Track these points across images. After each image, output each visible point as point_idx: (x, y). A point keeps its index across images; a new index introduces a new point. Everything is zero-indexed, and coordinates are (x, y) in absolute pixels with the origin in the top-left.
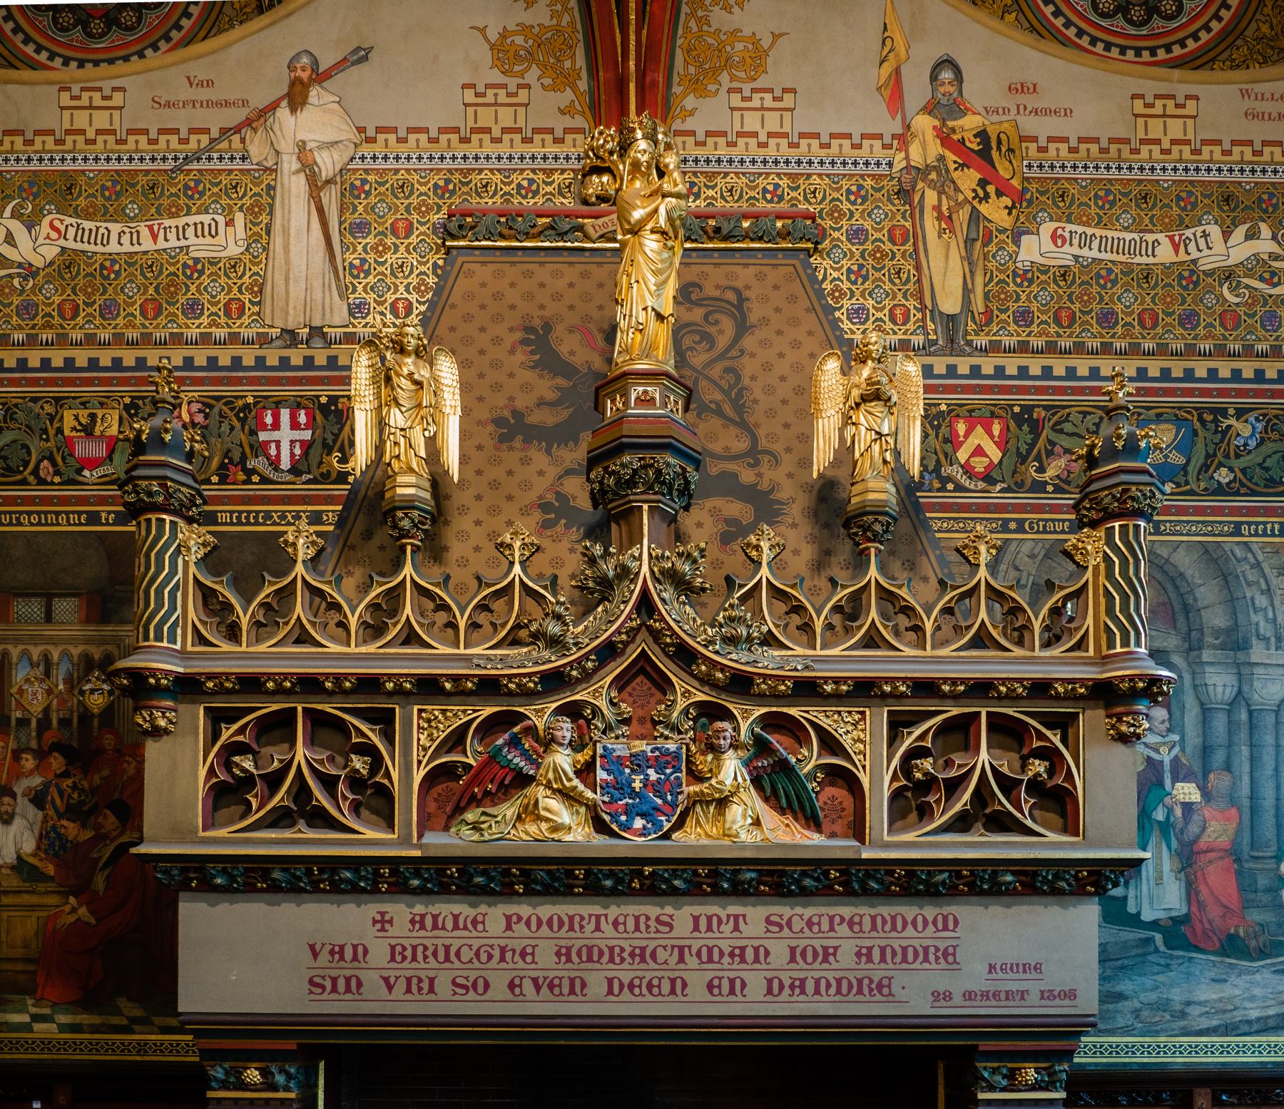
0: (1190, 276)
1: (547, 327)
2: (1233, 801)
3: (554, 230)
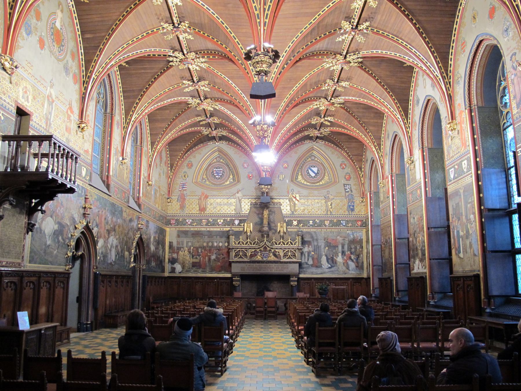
2: (317, 254)
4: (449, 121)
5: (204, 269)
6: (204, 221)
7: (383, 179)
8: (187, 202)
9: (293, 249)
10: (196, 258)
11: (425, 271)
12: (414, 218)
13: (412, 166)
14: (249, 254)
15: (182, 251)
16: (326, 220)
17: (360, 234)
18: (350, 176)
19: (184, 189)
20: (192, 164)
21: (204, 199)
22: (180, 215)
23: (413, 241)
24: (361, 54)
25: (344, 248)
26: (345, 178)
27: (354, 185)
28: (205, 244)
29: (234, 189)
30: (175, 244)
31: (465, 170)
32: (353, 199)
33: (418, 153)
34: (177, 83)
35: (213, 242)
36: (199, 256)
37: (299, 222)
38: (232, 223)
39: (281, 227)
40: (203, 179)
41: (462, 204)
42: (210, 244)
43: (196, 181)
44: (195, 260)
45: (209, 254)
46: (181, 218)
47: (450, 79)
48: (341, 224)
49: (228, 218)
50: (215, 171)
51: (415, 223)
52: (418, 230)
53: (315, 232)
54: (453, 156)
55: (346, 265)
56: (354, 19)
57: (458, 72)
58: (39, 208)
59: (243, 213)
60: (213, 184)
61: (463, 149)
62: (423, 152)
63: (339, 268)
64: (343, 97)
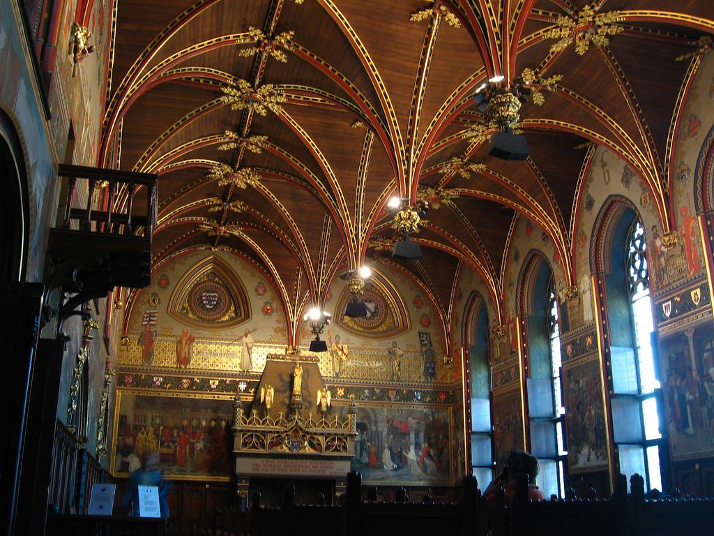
0: (370, 369)
1: (281, 374)
3: (282, 359)
4: (666, 230)
5: (183, 466)
6: (185, 381)
7: (502, 325)
8: (155, 345)
9: (343, 434)
10: (169, 447)
11: (604, 463)
12: (577, 382)
13: (575, 302)
14: (268, 441)
15: (143, 434)
16: (391, 390)
17: (445, 414)
18: (428, 319)
19: (151, 323)
20: (168, 280)
21: (186, 344)
22: (141, 368)
23: (573, 417)
24: (524, 123)
25: (418, 438)
26: (421, 322)
27: (435, 334)
28: (185, 423)
29: (239, 330)
30: (130, 419)
31: (697, 304)
32: (433, 357)
33: (589, 281)
34: (212, 132)
35: (199, 419)
36: (174, 442)
37: (348, 391)
38: (233, 387)
39: (324, 397)
40: (184, 308)
41: (690, 355)
42: (195, 423)
43: (173, 309)
44: (165, 450)
45: (191, 440)
46: (144, 374)
47: (667, 171)
48: (415, 396)
49: (228, 379)
50: (206, 296)
51: (579, 389)
52: (588, 399)
53: (372, 409)
54: (670, 284)
55: (421, 465)
56: (540, 68)
57: (682, 163)
58: (79, 308)
59: (253, 370)
60: (201, 318)
61: (692, 273)
62: (597, 279)
63: (410, 470)
64: (460, 190)
